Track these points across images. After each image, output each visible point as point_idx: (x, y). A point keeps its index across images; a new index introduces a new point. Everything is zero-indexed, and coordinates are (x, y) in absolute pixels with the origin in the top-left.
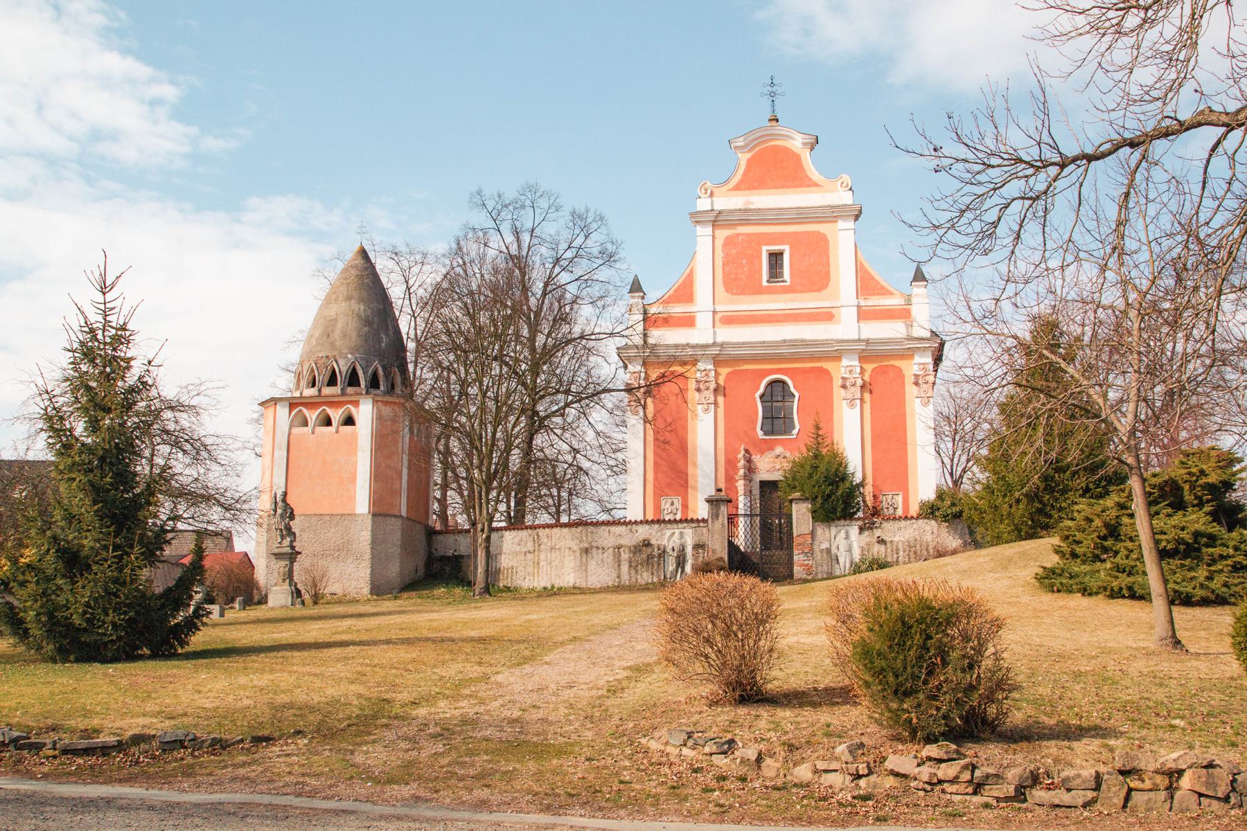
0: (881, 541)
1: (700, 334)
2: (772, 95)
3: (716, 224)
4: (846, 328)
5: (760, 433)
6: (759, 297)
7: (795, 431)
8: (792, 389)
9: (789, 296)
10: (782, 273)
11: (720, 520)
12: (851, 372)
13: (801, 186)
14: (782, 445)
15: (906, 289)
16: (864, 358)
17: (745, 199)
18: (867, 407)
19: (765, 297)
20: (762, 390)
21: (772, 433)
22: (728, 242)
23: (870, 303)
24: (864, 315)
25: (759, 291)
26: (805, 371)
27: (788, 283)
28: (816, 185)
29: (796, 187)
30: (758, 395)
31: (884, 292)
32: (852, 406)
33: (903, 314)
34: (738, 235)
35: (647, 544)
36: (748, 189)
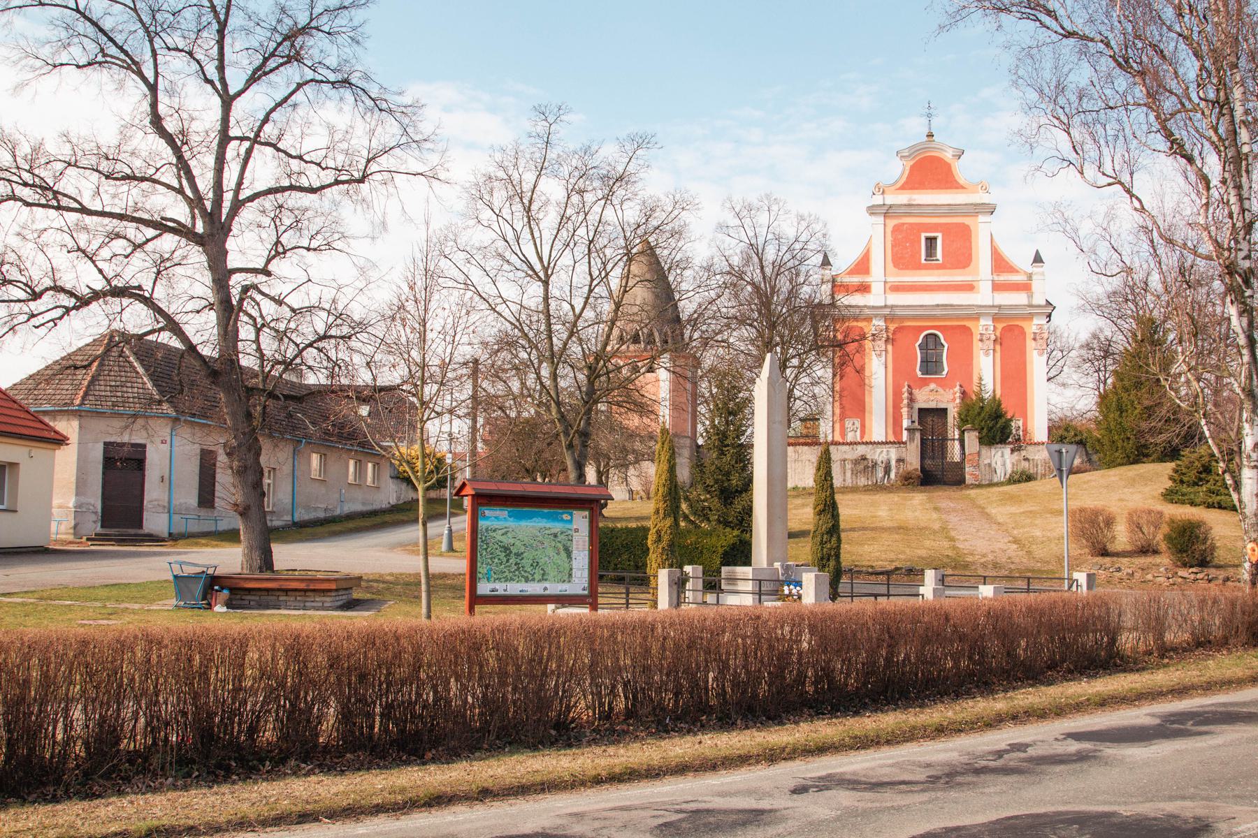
0: (1026, 459)
1: (875, 298)
2: (929, 115)
3: (886, 215)
4: (984, 296)
5: (919, 373)
6: (918, 272)
7: (945, 373)
8: (943, 341)
9: (941, 271)
10: (935, 253)
12: (986, 329)
15: (1030, 269)
16: (996, 318)
18: (998, 355)
19: (923, 272)
21: (927, 374)
22: (897, 229)
23: (1002, 278)
24: (997, 287)
25: (919, 267)
26: (953, 327)
27: (941, 262)
30: (917, 345)
32: (987, 354)
33: (1025, 287)
35: (864, 458)
36: (911, 189)
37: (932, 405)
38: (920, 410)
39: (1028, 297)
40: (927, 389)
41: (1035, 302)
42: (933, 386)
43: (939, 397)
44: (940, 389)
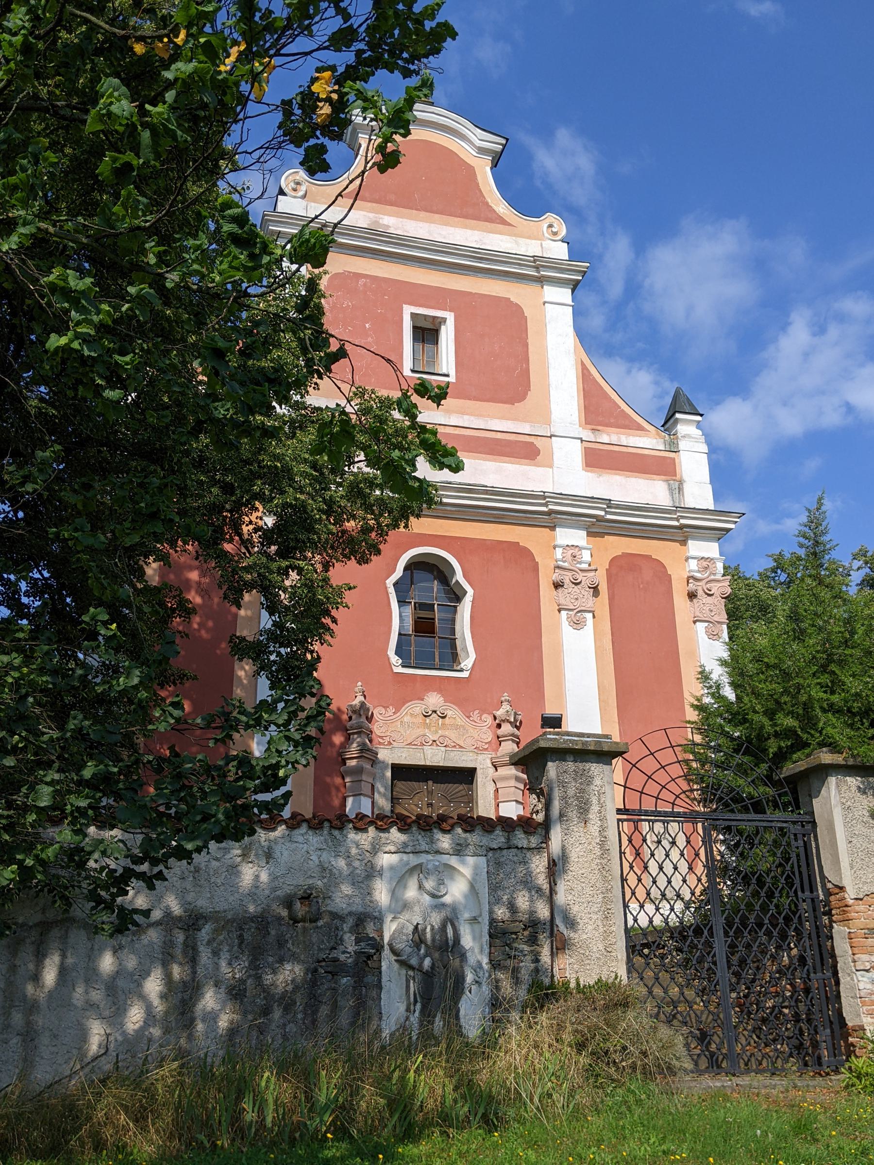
5: (395, 659)
11: (594, 828)
13: (477, 218)
14: (440, 691)
17: (371, 215)
20: (399, 572)
23: (605, 439)
28: (504, 222)
29: (466, 217)
31: (628, 425)
32: (577, 624)
34: (358, 276)
37: (434, 757)
38: (402, 772)
39: (671, 490)
40: (417, 707)
41: (690, 501)
42: (434, 700)
43: (452, 734)
44: (454, 713)
